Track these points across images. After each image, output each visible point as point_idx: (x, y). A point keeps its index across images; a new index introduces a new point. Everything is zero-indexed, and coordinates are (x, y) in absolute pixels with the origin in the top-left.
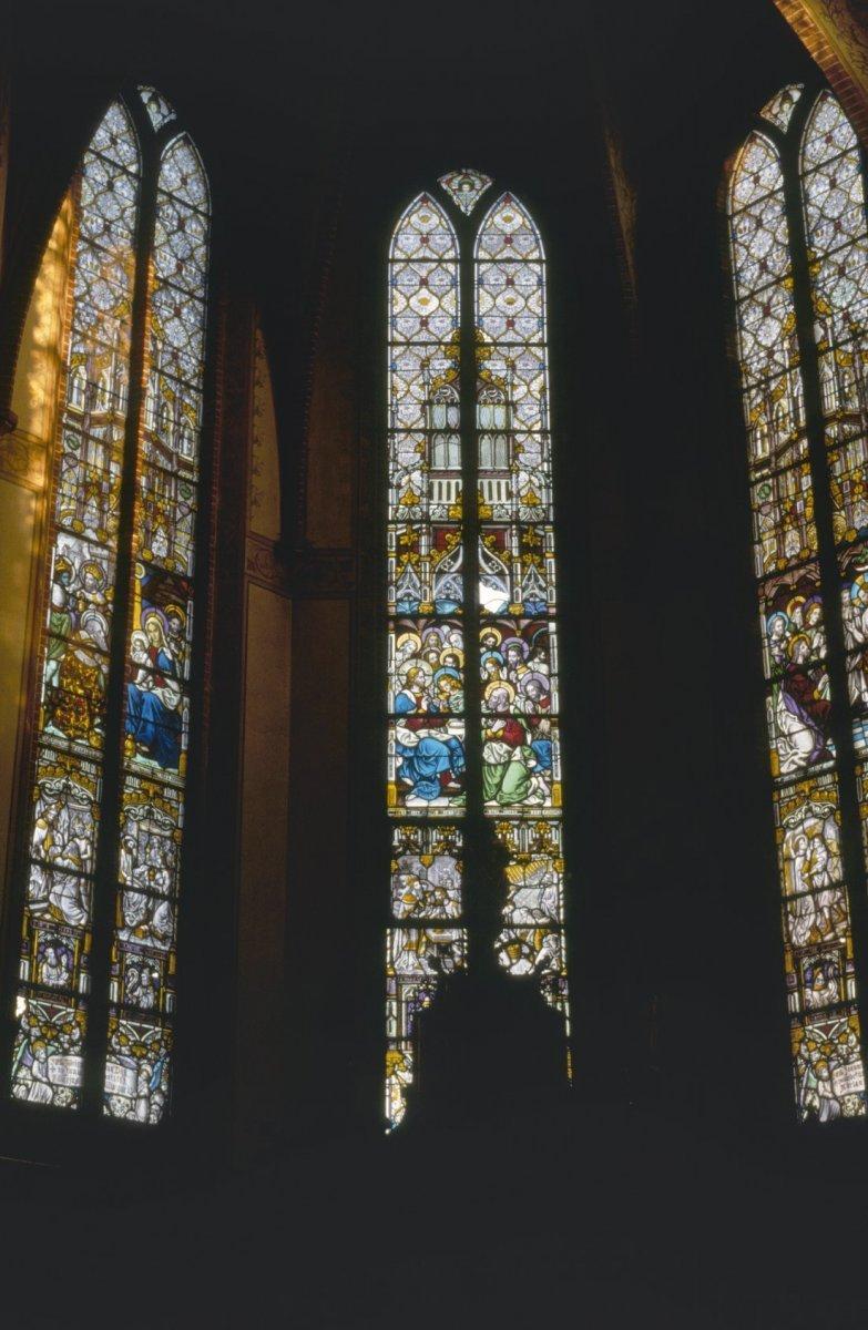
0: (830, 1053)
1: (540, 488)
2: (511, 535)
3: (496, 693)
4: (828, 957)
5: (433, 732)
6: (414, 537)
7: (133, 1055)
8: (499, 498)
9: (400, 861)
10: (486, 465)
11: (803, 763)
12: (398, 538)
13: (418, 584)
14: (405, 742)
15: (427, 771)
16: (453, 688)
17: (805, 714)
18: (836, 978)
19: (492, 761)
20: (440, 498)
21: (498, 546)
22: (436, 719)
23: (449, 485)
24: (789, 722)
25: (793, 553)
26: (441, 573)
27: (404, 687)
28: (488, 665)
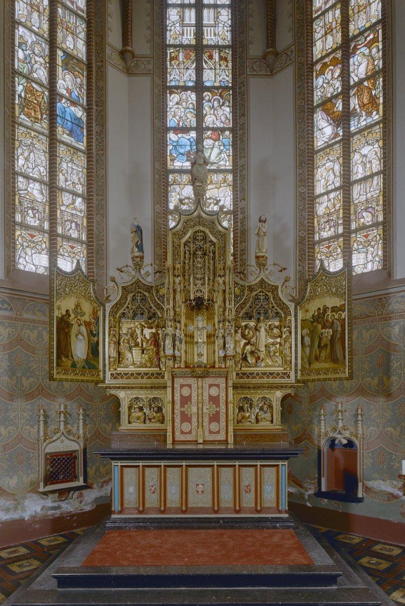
0: (329, 255)
1: (227, 31)
2: (216, 53)
3: (209, 120)
4: (331, 218)
5: (184, 135)
6: (176, 53)
7: (69, 256)
8: (211, 36)
9: (172, 187)
10: (205, 22)
11: (327, 140)
12: (170, 53)
13: (180, 73)
14: (173, 139)
15: (182, 151)
16: (192, 117)
17: (329, 118)
18: (334, 226)
19: (207, 147)
20: (187, 36)
21: (211, 57)
22: (185, 130)
23: (190, 30)
24: (323, 123)
25: (330, 47)
26: (188, 69)
27: (173, 117)
28: (206, 108)
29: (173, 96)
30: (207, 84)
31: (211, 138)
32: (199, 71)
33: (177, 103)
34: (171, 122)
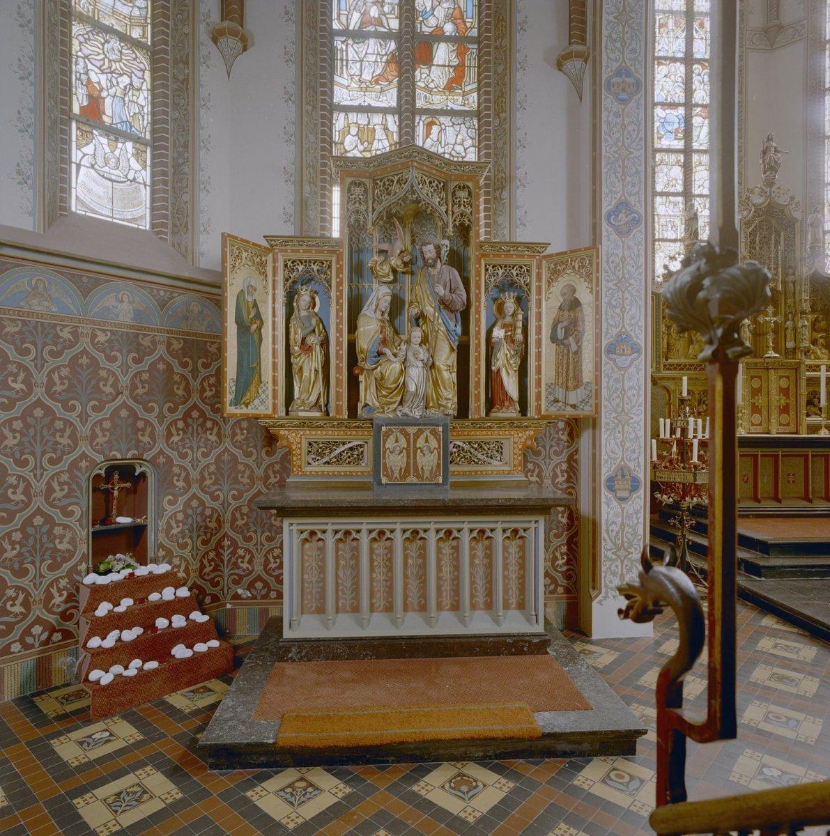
15: (670, 128)
22: (673, 105)
29: (661, 67)
30: (697, 56)
31: (700, 115)
32: (689, 41)
33: (666, 76)
34: (659, 97)
